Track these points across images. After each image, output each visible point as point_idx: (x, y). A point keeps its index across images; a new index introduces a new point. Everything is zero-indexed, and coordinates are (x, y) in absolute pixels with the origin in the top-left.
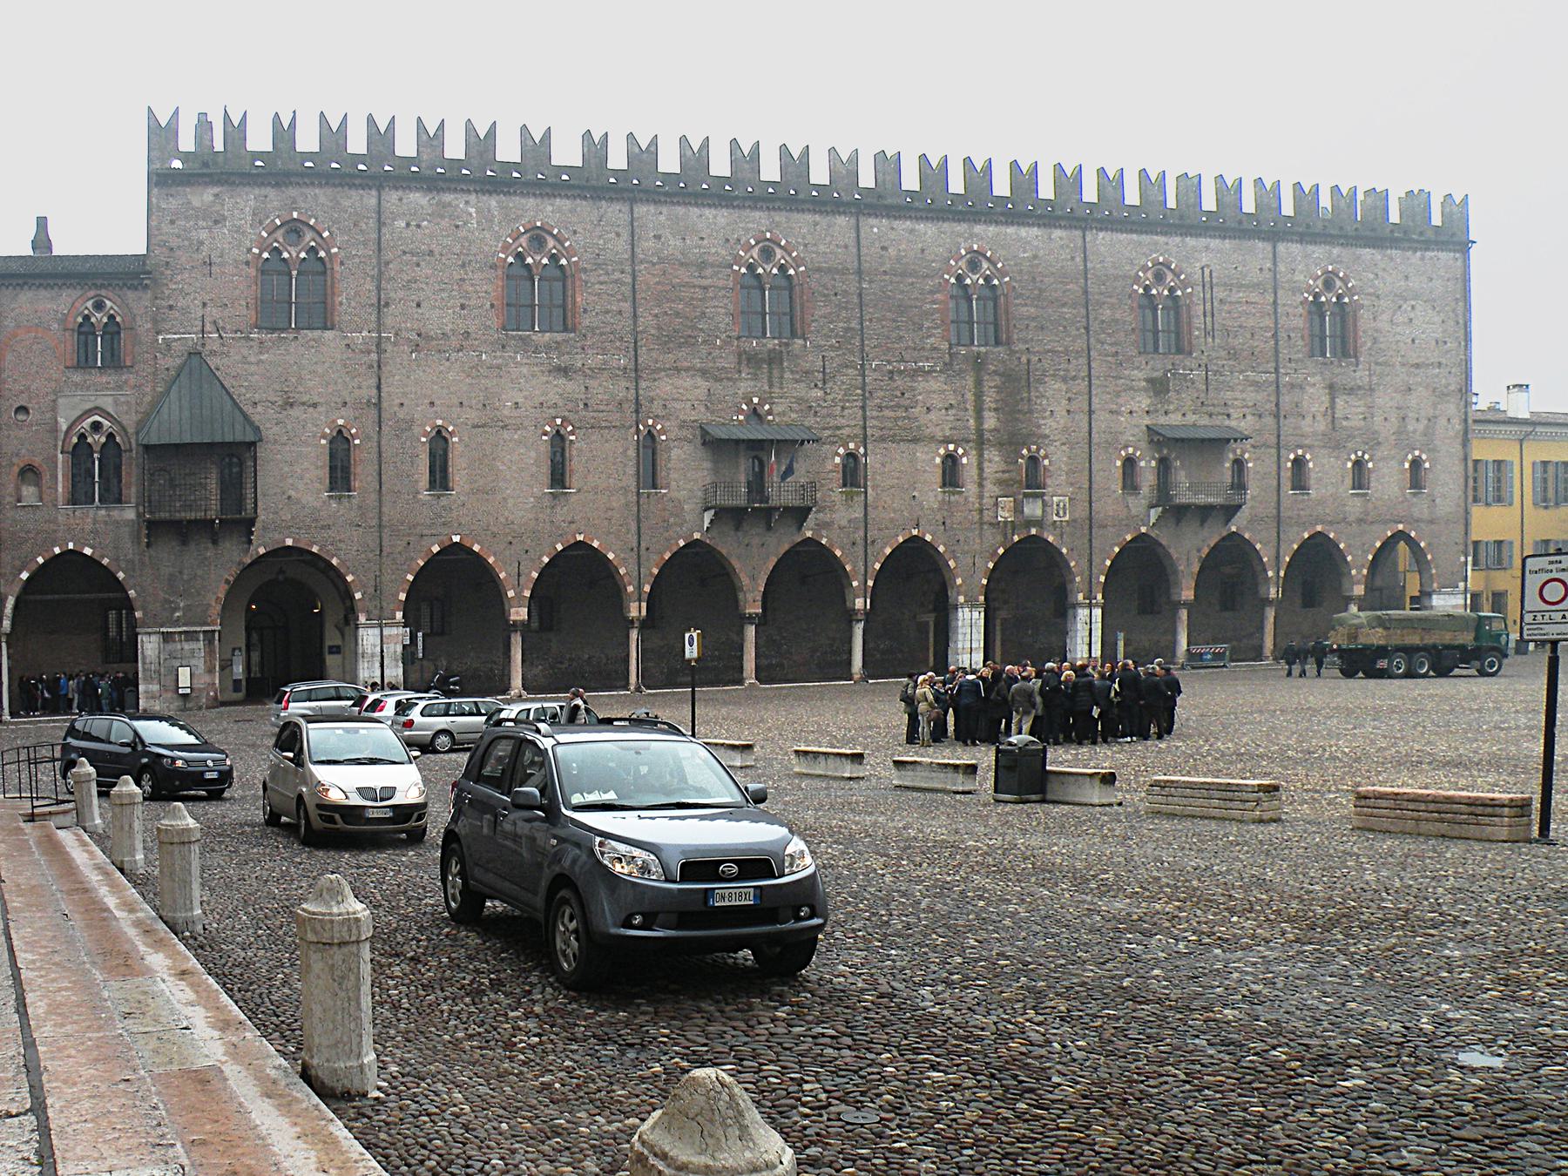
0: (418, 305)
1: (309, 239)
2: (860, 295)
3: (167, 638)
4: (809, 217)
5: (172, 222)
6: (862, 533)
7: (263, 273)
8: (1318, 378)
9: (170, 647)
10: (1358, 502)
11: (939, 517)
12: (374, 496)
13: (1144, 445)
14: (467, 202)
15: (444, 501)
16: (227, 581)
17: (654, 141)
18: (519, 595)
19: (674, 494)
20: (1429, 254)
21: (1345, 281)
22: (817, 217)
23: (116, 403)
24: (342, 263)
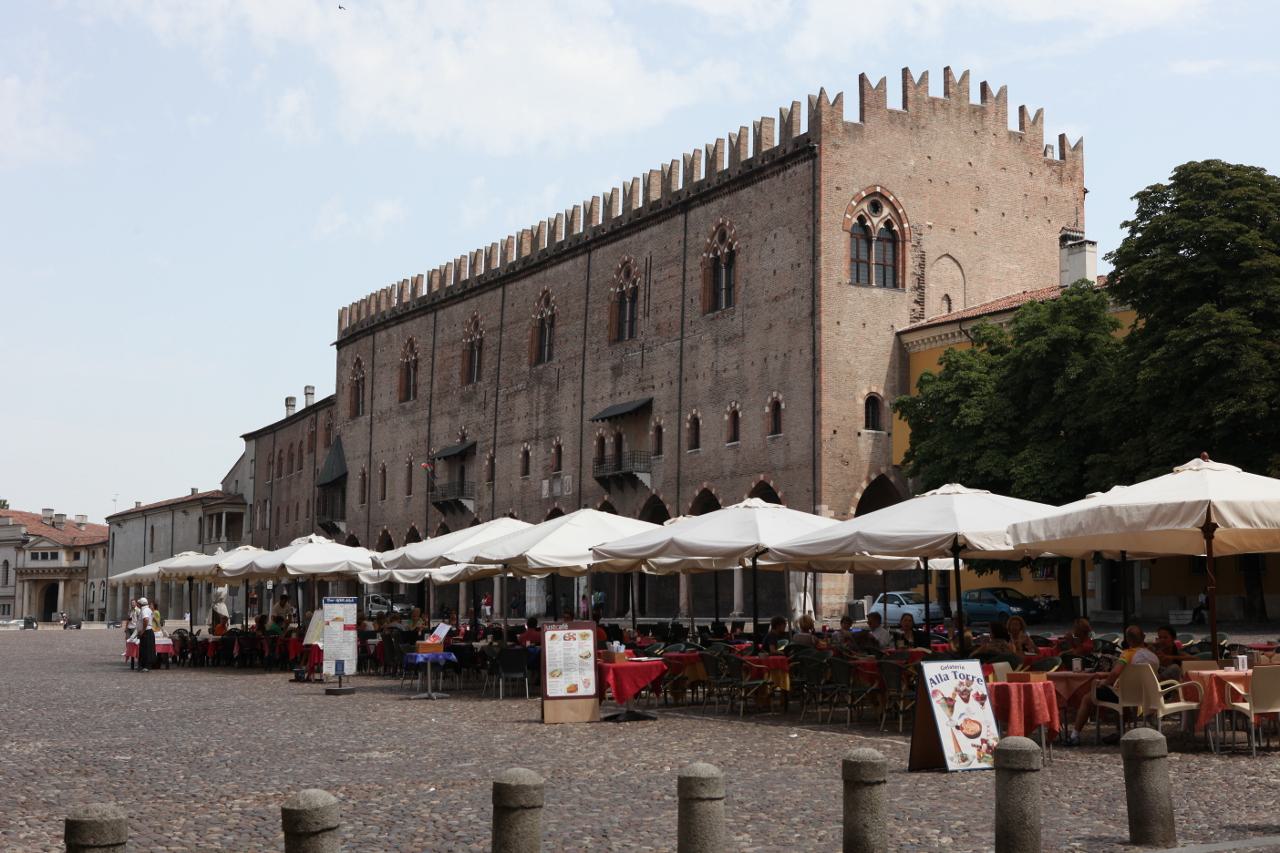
8: (709, 334)
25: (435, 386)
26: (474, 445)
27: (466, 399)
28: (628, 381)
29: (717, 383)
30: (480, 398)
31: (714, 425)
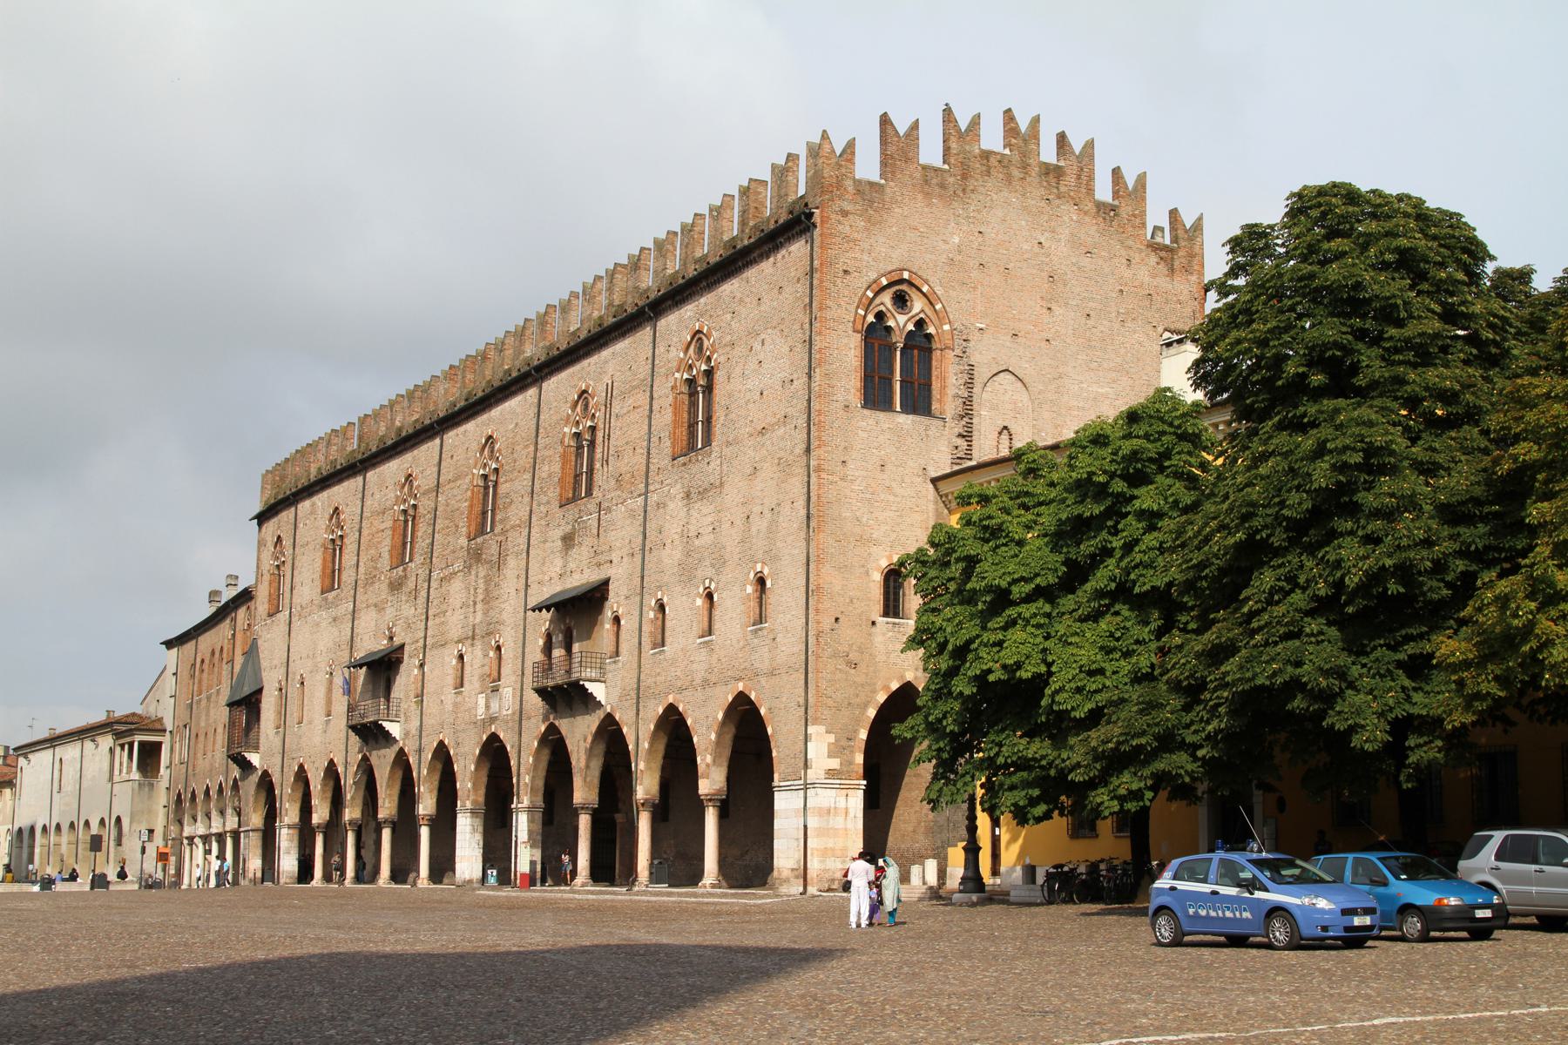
10: (702, 655)
25: (362, 569)
26: (402, 647)
27: (396, 586)
28: (581, 553)
29: (688, 555)
30: (411, 584)
31: (684, 609)
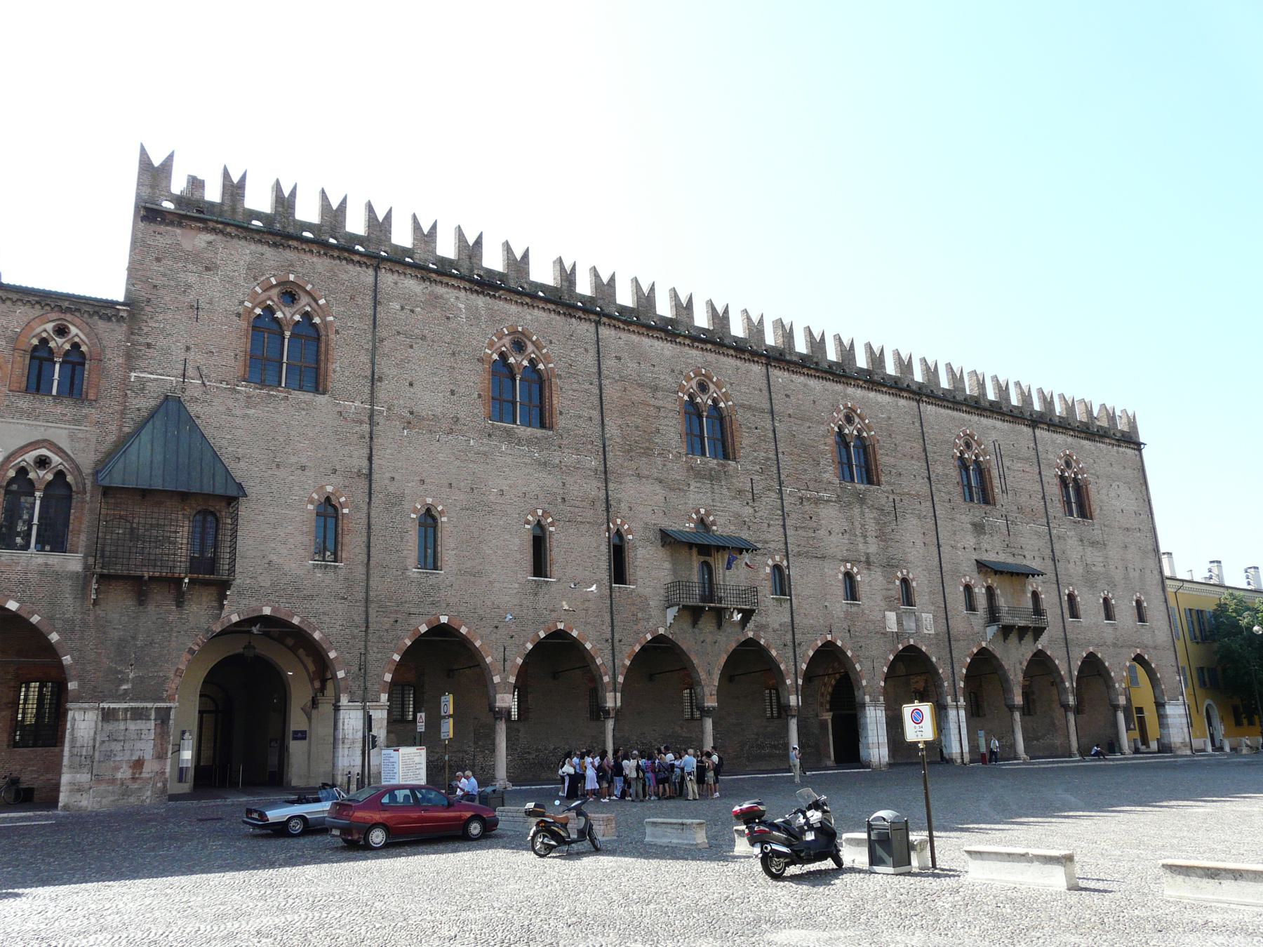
0: (411, 385)
1: (304, 303)
2: (774, 431)
3: (108, 716)
4: (732, 361)
5: (158, 260)
6: (789, 636)
7: (254, 328)
9: (110, 727)
10: (1110, 630)
11: (845, 626)
12: (362, 569)
13: (975, 574)
14: (457, 298)
15: (432, 580)
16: (191, 651)
17: (612, 279)
18: (504, 680)
19: (640, 590)
20: (1121, 449)
21: (1077, 462)
22: (738, 363)
23: (72, 437)
24: (337, 332)
31: (1090, 604)
